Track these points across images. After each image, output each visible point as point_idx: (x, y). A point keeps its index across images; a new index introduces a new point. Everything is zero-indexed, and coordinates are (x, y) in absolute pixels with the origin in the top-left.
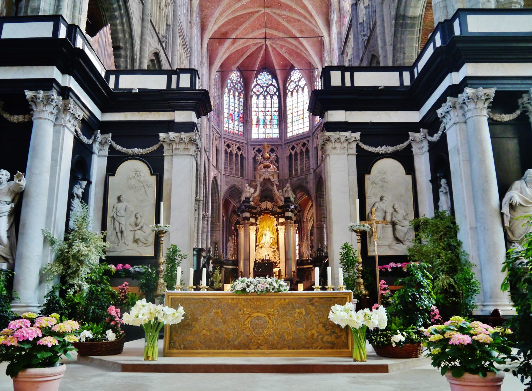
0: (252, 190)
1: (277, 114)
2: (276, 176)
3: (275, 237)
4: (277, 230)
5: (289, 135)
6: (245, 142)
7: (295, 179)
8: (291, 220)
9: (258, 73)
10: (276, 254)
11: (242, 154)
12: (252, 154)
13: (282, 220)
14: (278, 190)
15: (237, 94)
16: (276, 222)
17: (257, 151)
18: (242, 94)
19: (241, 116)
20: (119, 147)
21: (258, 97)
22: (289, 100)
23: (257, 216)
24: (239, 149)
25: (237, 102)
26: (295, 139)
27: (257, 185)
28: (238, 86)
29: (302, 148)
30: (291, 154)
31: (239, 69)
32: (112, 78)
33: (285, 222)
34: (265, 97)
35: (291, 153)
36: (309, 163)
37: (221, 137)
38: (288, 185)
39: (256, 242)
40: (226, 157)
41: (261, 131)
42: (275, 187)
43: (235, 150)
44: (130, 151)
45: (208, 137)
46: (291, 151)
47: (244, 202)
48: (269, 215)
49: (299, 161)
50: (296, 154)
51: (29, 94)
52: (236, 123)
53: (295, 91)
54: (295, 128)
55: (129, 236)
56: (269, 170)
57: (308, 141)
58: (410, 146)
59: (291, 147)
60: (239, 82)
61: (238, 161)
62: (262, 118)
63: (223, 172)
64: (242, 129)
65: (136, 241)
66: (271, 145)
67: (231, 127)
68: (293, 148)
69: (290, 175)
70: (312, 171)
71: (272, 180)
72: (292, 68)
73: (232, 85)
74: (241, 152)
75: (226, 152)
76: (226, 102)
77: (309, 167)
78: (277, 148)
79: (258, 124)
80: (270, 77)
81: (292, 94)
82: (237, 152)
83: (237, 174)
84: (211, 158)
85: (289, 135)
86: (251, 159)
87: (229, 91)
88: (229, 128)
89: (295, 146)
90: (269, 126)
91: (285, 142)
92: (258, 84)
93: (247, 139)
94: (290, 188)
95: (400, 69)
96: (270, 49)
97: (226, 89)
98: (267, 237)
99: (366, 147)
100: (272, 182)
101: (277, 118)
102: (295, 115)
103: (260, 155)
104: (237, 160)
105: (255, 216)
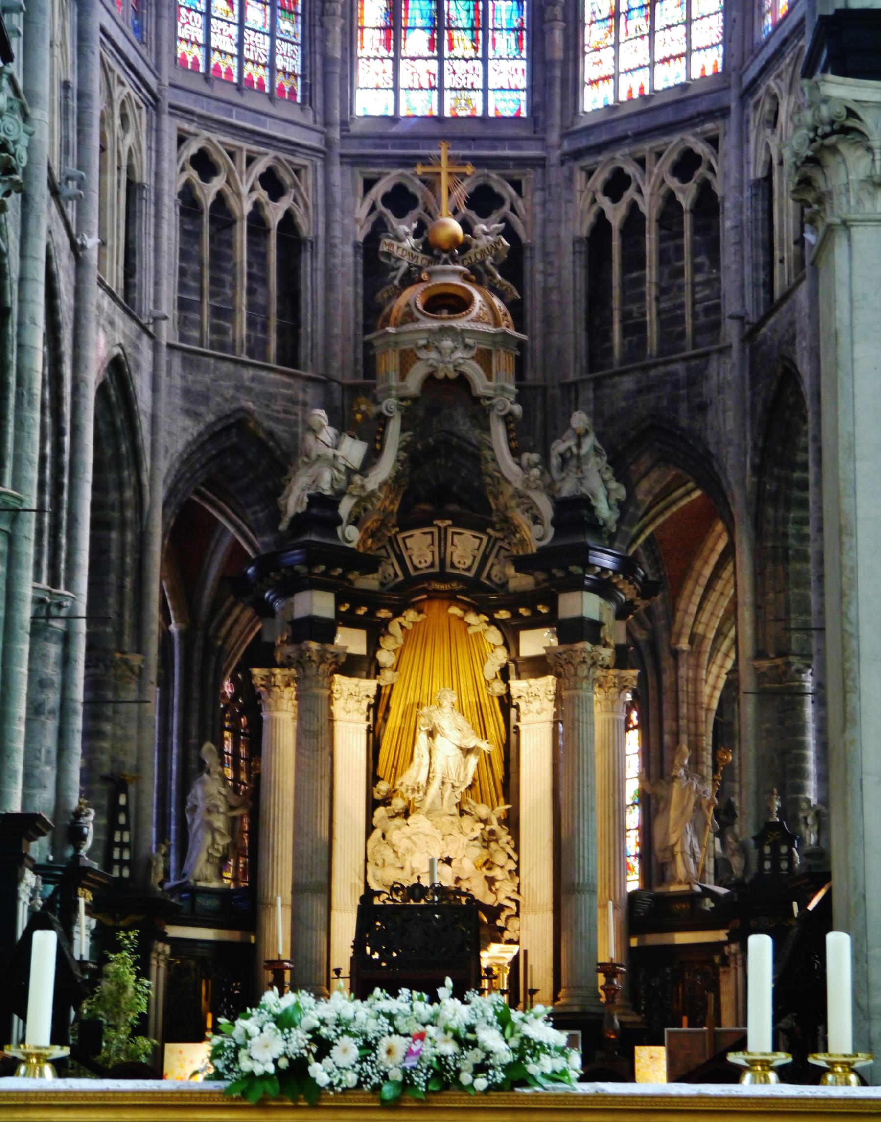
2: (503, 363)
4: (506, 703)
6: (313, 140)
7: (628, 383)
8: (596, 640)
10: (500, 859)
11: (288, 221)
14: (516, 453)
16: (501, 656)
17: (387, 199)
23: (384, 613)
26: (630, 128)
27: (383, 420)
29: (674, 183)
30: (601, 222)
33: (558, 656)
35: (601, 214)
36: (714, 283)
37: (154, 103)
38: (580, 420)
39: (373, 778)
40: (190, 236)
42: (499, 434)
43: (244, 189)
45: (73, 104)
46: (605, 202)
47: (300, 522)
48: (455, 610)
49: (651, 273)
50: (634, 217)
56: (460, 323)
57: (713, 142)
59: (601, 177)
61: (264, 267)
63: (167, 333)
66: (478, 162)
70: (731, 332)
71: (481, 384)
74: (285, 203)
77: (717, 308)
78: (517, 185)
82: (257, 205)
83: (257, 348)
84: (92, 242)
86: (349, 249)
88: (208, 48)
89: (631, 169)
90: (463, 43)
91: (566, 146)
93: (327, 123)
94: (589, 442)
100: (477, 400)
103: (405, 227)
104: (257, 254)
105: (371, 613)
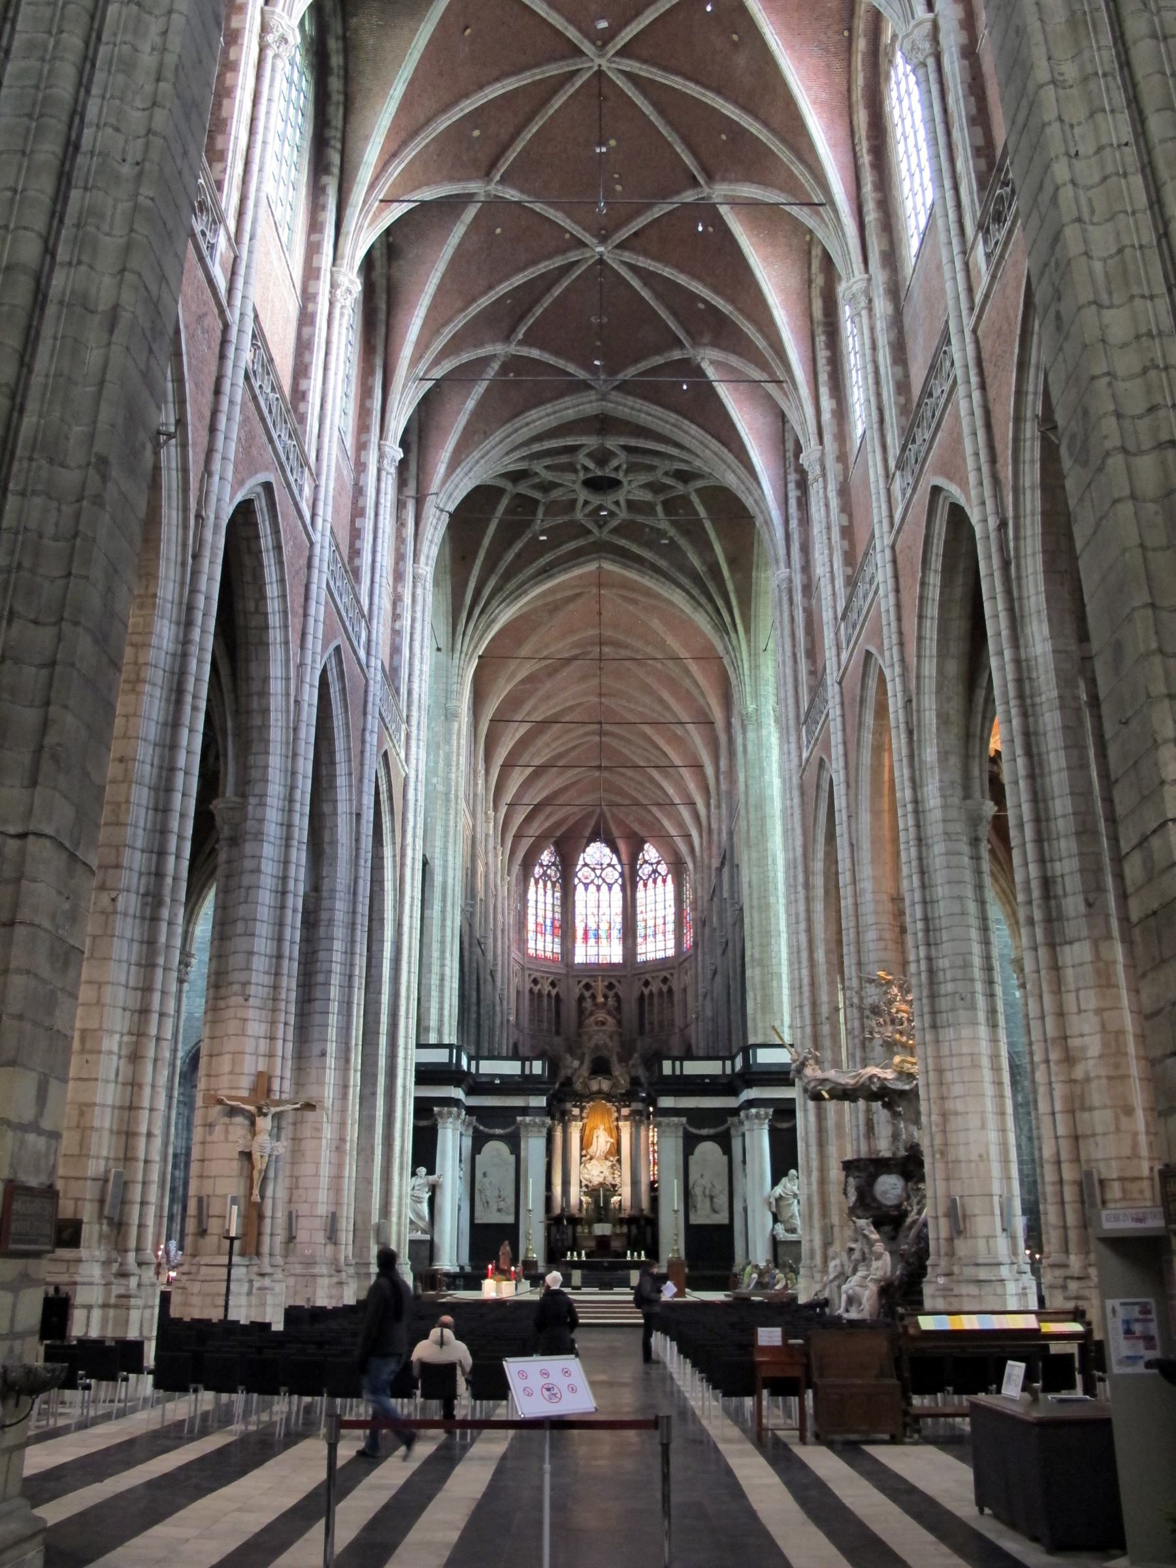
0: (576, 1063)
1: (619, 919)
4: (618, 1128)
5: (640, 958)
9: (588, 845)
11: (557, 995)
12: (577, 991)
13: (625, 1111)
15: (549, 884)
19: (557, 924)
21: (586, 886)
22: (640, 894)
24: (553, 984)
25: (549, 900)
27: (583, 1054)
30: (642, 996)
31: (557, 844)
32: (473, 1063)
34: (598, 888)
39: (582, 1149)
40: (531, 1000)
41: (592, 951)
50: (651, 994)
52: (549, 938)
54: (651, 946)
55: (494, 1207)
60: (554, 864)
62: (594, 927)
64: (557, 949)
65: (499, 1210)
67: (540, 946)
69: (641, 1031)
75: (531, 991)
76: (531, 904)
79: (586, 937)
80: (607, 851)
81: (645, 885)
87: (537, 883)
92: (586, 865)
95: (723, 1059)
96: (608, 815)
98: (602, 1141)
101: (619, 926)
102: (651, 923)
104: (549, 1004)
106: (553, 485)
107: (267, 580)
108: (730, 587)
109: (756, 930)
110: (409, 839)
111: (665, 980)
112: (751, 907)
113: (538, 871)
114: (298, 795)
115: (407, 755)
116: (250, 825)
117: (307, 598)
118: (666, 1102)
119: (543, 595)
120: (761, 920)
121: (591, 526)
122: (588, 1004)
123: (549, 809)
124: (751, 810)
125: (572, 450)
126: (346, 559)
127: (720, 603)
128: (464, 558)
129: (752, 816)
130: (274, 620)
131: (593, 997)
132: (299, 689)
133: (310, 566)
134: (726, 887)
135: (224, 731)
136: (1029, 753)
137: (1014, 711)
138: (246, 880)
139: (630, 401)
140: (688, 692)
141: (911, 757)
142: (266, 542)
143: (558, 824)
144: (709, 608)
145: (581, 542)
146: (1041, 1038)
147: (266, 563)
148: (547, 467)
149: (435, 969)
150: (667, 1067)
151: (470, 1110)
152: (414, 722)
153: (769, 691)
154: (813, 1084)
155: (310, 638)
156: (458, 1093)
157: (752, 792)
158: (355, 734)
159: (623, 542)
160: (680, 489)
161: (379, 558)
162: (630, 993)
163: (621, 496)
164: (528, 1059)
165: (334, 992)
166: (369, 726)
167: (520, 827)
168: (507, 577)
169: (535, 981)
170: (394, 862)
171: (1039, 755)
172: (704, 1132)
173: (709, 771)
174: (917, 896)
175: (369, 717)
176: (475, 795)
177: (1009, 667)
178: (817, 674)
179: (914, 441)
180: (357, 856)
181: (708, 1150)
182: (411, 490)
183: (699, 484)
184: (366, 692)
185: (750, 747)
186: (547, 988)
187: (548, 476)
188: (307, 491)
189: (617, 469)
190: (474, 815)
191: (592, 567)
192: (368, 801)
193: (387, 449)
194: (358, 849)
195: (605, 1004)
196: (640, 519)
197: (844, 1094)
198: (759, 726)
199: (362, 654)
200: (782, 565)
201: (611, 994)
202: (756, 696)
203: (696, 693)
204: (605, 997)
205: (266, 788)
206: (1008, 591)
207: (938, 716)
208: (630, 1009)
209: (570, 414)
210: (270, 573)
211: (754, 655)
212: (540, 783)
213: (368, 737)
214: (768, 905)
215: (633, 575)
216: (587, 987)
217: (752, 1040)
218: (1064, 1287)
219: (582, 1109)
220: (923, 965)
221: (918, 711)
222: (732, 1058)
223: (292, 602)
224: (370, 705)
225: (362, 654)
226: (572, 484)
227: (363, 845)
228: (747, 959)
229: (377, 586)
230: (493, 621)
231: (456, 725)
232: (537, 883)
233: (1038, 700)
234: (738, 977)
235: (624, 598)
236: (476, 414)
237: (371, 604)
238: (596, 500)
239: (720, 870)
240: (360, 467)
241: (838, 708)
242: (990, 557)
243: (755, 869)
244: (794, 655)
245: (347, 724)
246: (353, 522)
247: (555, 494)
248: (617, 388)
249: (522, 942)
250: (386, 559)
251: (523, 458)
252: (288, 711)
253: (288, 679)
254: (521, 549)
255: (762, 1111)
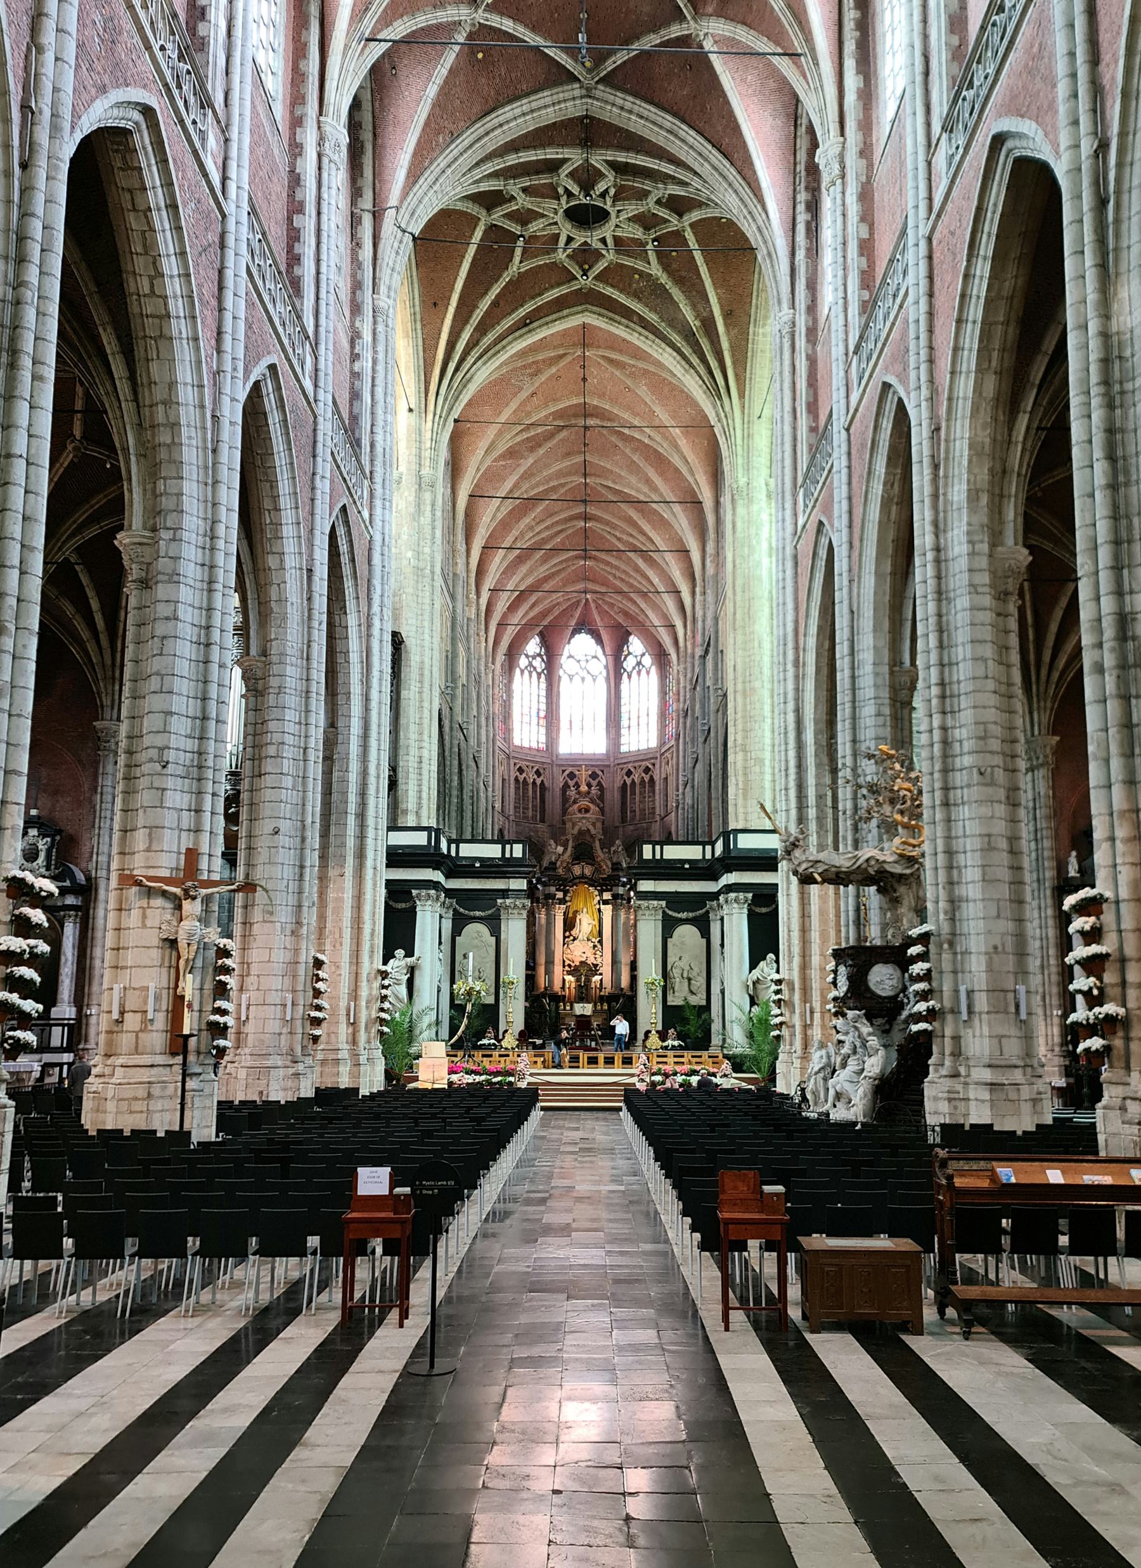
0: (560, 849)
3: (596, 923)
5: (624, 749)
7: (631, 827)
12: (560, 781)
13: (607, 896)
15: (534, 674)
18: (543, 676)
19: (542, 714)
20: (462, 910)
21: (571, 677)
22: (625, 685)
24: (538, 773)
26: (632, 759)
28: (538, 664)
31: (541, 635)
32: (453, 846)
34: (583, 679)
36: (654, 801)
39: (565, 931)
40: (517, 789)
44: (472, 913)
51: (415, 892)
53: (635, 672)
58: (708, 912)
59: (625, 771)
60: (539, 655)
64: (543, 739)
68: (629, 773)
69: (623, 819)
72: (629, 634)
73: (527, 663)
75: (517, 779)
80: (593, 641)
81: (629, 677)
83: (534, 817)
85: (624, 749)
87: (522, 672)
92: (570, 656)
95: (704, 844)
96: (593, 605)
97: (518, 671)
98: (585, 924)
99: (670, 913)
104: (534, 792)
106: (535, 215)
107: (163, 251)
108: (725, 345)
109: (739, 715)
110: (376, 609)
111: (647, 770)
112: (735, 692)
113: (523, 662)
114: (221, 530)
115: (371, 515)
116: (163, 564)
117: (221, 288)
118: (645, 886)
119: (522, 354)
120: (745, 705)
121: (575, 271)
122: (572, 792)
123: (533, 598)
124: (739, 590)
125: (553, 166)
126: (283, 268)
127: (713, 364)
128: (435, 304)
129: (739, 598)
130: (177, 307)
131: (577, 785)
132: (216, 402)
133: (223, 246)
134: (709, 674)
135: (126, 450)
136: (1111, 457)
137: (1095, 402)
138: (161, 629)
139: (619, 98)
140: (677, 470)
141: (935, 496)
142: (156, 197)
143: (544, 614)
144: (702, 370)
145: (564, 290)
146: (1104, 810)
147: (157, 226)
148: (524, 190)
149: (413, 751)
150: (647, 852)
151: (450, 893)
152: (378, 479)
153: (761, 461)
154: (804, 866)
155: (227, 339)
156: (437, 876)
157: (739, 572)
158: (302, 480)
159: (609, 291)
160: (674, 223)
161: (323, 269)
162: (613, 782)
163: (607, 231)
164: (508, 842)
165: (287, 766)
166: (319, 470)
167: (504, 616)
168: (482, 329)
169: (521, 770)
170: (360, 631)
171: (1125, 458)
172: (683, 915)
173: (696, 556)
174: (934, 658)
175: (319, 460)
176: (455, 574)
177: (1094, 344)
178: (820, 434)
179: (971, 86)
180: (310, 618)
181: (687, 934)
182: (366, 202)
183: (695, 215)
184: (315, 430)
185: (739, 524)
186: (531, 777)
187: (523, 202)
188: (213, 141)
189: (603, 195)
190: (453, 597)
191: (573, 321)
192: (322, 556)
193: (327, 129)
194: (310, 610)
195: (589, 793)
196: (628, 262)
197: (837, 878)
198: (750, 500)
199: (308, 384)
200: (785, 305)
201: (594, 783)
202: (748, 468)
203: (684, 470)
204: (589, 785)
205: (181, 521)
206: (1101, 240)
207: (971, 447)
208: (613, 797)
209: (550, 116)
210: (166, 243)
211: (747, 423)
212: (523, 569)
213: (318, 483)
214: (753, 689)
215: (620, 331)
216: (572, 776)
217: (732, 826)
218: (1123, 1109)
219: (566, 893)
220: (937, 735)
221: (947, 441)
222: (713, 844)
223: (200, 286)
224: (320, 446)
225: (308, 384)
226: (553, 212)
227: (316, 605)
228: (730, 744)
229: (323, 303)
230: (469, 381)
231: (427, 496)
232: (522, 672)
233: (1129, 386)
234: (720, 766)
235: (611, 361)
236: (440, 104)
237: (317, 326)
238: (581, 237)
239: (704, 657)
240: (296, 149)
241: (844, 458)
242: (1079, 197)
243: (740, 652)
244: (794, 410)
245: (292, 464)
246: (290, 220)
247: (535, 227)
248: (606, 80)
249: (508, 731)
250: (336, 277)
251: (495, 175)
252: (204, 428)
253: (201, 386)
254: (498, 296)
255: (741, 896)
